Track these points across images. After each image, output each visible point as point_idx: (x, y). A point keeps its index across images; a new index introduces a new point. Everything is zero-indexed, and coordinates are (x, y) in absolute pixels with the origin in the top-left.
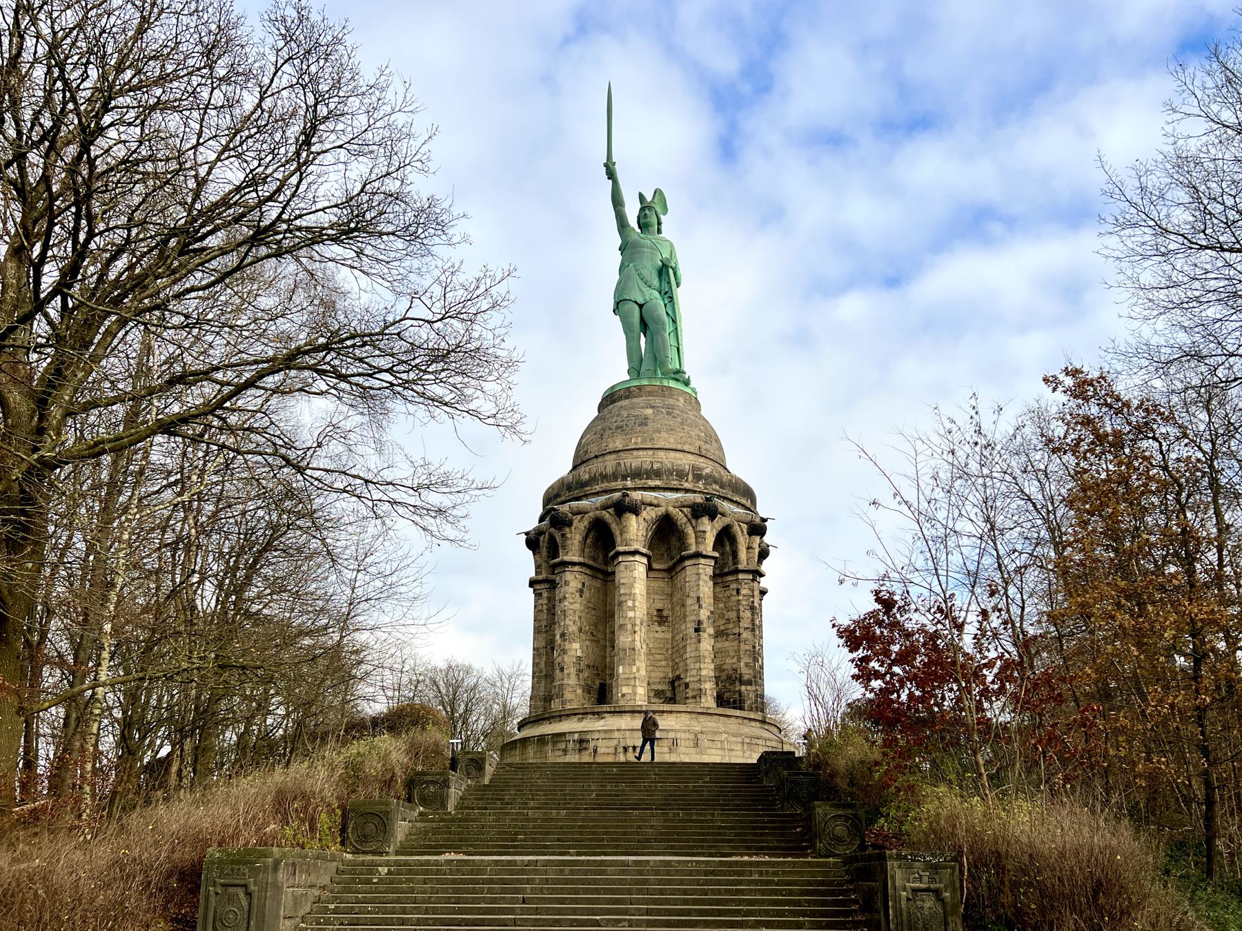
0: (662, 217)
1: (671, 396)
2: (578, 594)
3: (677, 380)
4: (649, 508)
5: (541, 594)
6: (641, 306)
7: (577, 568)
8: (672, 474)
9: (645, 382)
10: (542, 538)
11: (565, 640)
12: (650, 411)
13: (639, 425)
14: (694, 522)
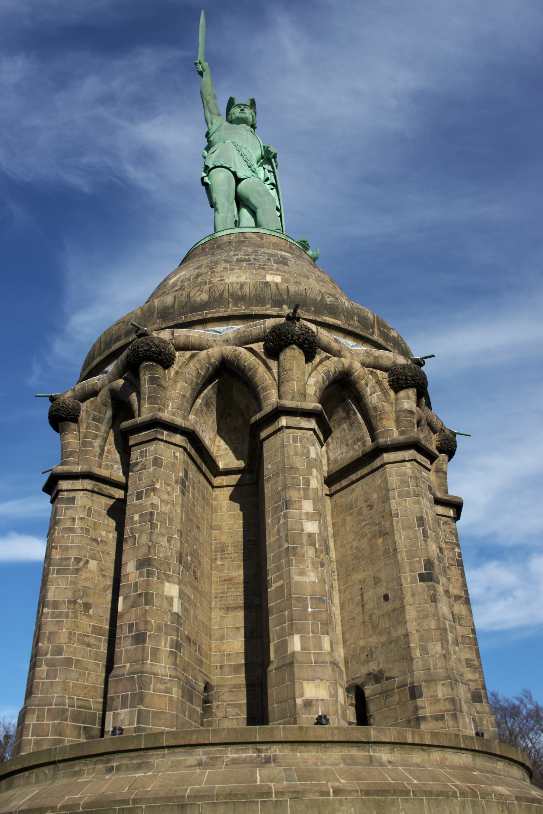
2: (178, 487)
4: (324, 354)
5: (72, 500)
6: (238, 181)
7: (178, 439)
8: (352, 318)
10: (84, 406)
11: (149, 574)
13: (276, 262)
14: (392, 393)
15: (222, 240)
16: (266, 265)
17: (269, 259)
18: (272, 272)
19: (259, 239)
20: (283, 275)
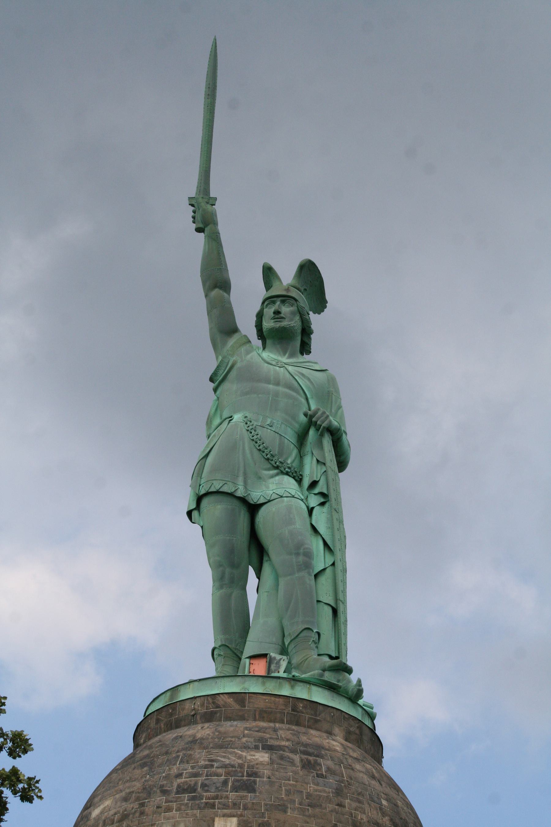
0: (313, 317)
1: (314, 724)
3: (332, 688)
9: (255, 687)
12: (262, 757)
13: (235, 789)
15: (183, 709)
16: (217, 797)
17: (225, 783)
18: (225, 811)
19: (237, 707)
20: (241, 815)
